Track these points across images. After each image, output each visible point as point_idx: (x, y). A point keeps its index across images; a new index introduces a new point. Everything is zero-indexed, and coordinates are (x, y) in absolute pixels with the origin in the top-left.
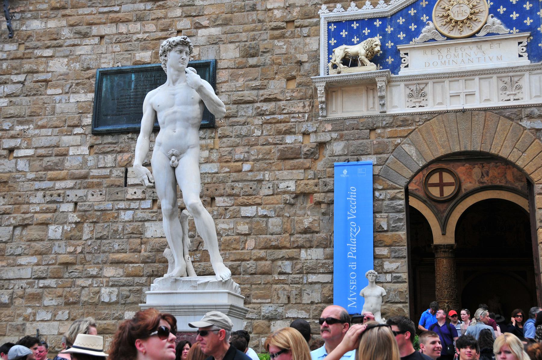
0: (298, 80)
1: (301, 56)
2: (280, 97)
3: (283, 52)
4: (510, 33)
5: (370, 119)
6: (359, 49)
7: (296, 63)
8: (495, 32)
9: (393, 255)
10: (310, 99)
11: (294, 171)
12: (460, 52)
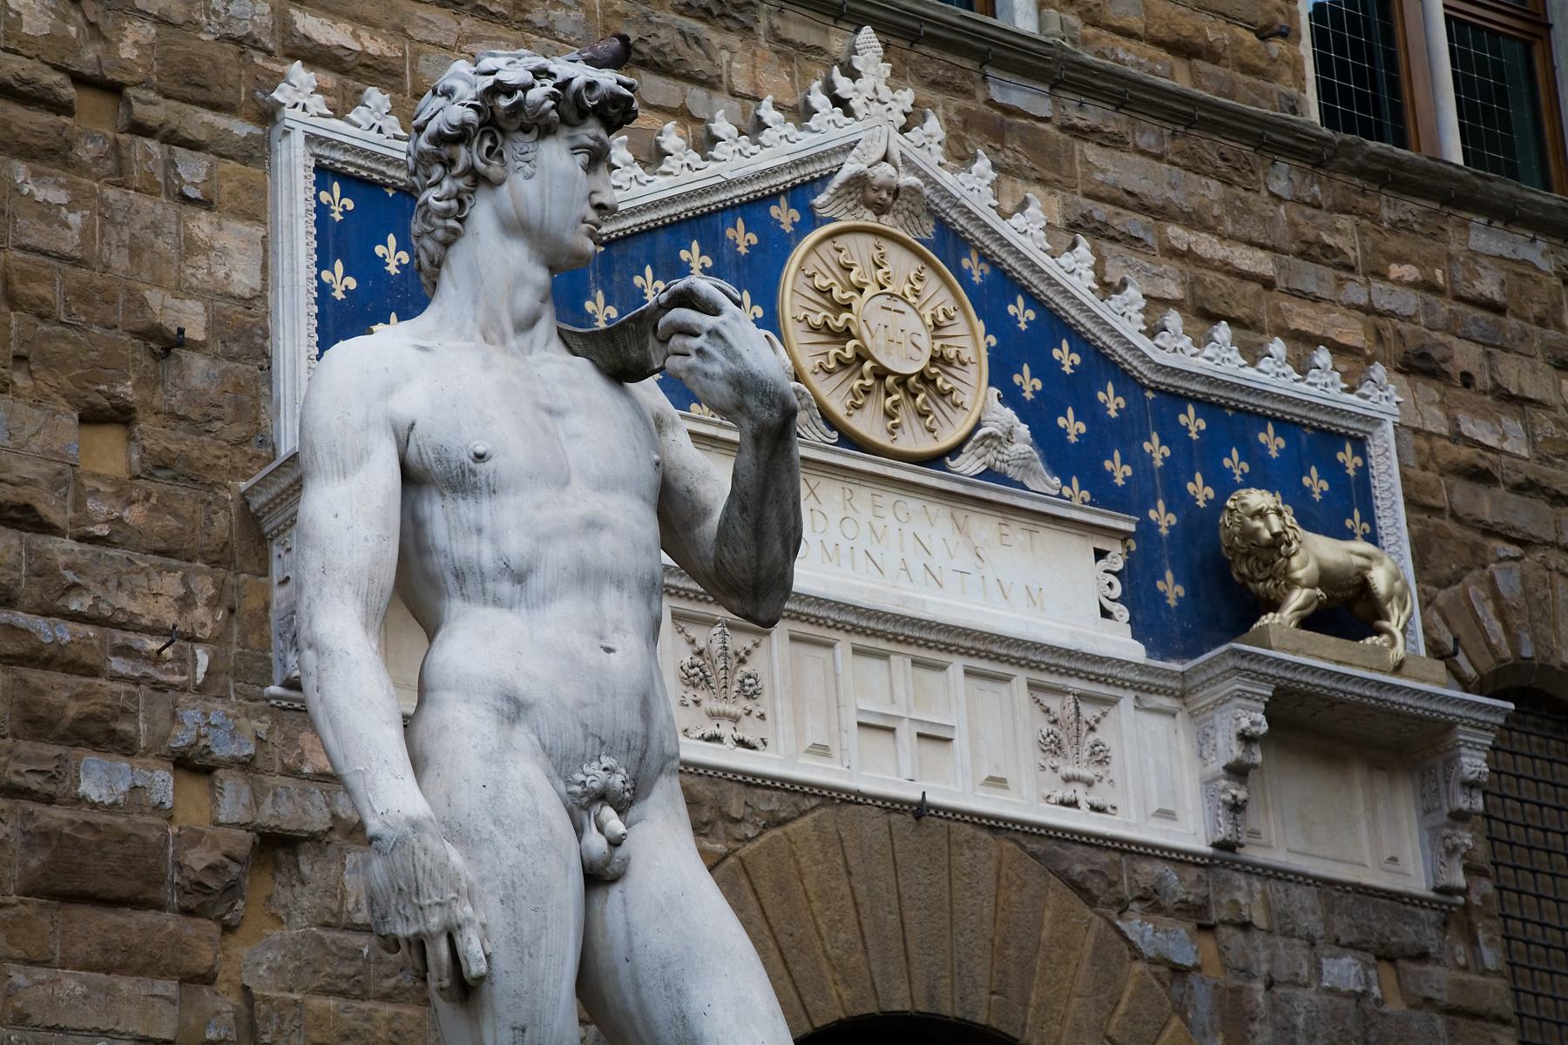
0: (154, 434)
1: (169, 301)
2: (52, 508)
3: (66, 248)
4: (1060, 496)
7: (137, 334)
8: (1012, 472)
10: (215, 564)
11: (125, 984)
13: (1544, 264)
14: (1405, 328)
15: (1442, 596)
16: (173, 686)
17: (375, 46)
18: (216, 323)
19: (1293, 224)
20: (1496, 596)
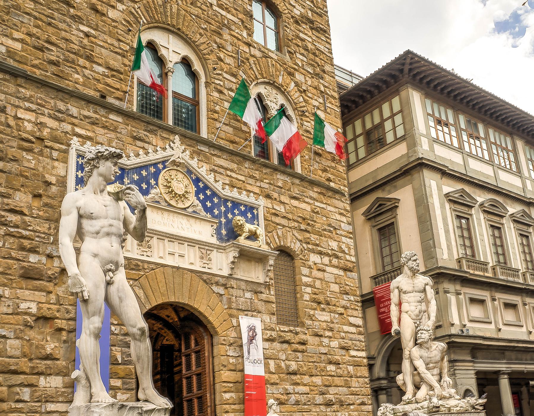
0: (45, 200)
1: (49, 177)
2: (26, 211)
3: (32, 167)
12: (176, 220)
13: (289, 181)
14: (266, 190)
15: (269, 235)
16: (46, 243)
17: (90, 134)
18: (57, 181)
19: (248, 172)
20: (278, 235)
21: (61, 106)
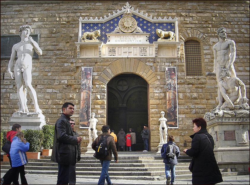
0: (70, 43)
5: (95, 59)
6: (92, 33)
9: (101, 108)
11: (67, 77)
21: (76, 7)
